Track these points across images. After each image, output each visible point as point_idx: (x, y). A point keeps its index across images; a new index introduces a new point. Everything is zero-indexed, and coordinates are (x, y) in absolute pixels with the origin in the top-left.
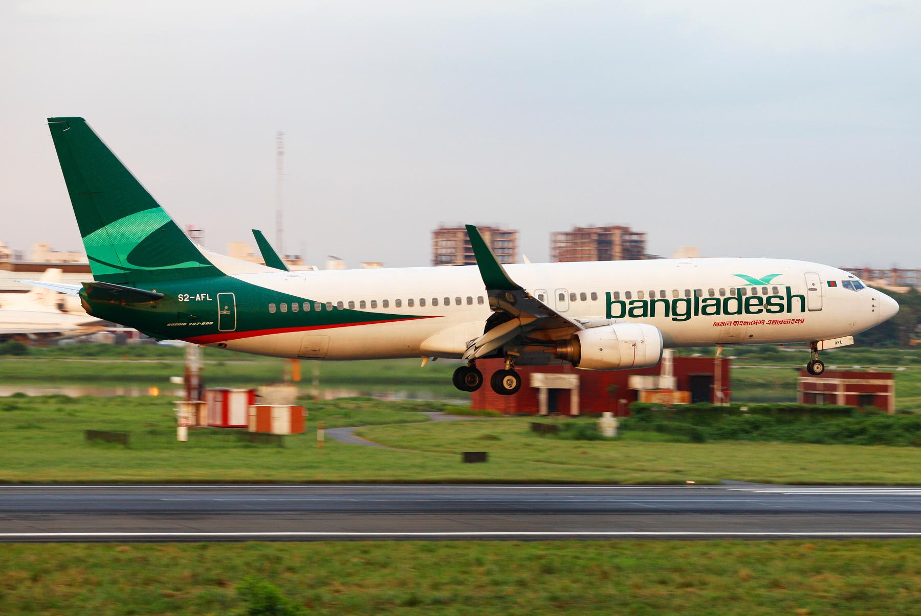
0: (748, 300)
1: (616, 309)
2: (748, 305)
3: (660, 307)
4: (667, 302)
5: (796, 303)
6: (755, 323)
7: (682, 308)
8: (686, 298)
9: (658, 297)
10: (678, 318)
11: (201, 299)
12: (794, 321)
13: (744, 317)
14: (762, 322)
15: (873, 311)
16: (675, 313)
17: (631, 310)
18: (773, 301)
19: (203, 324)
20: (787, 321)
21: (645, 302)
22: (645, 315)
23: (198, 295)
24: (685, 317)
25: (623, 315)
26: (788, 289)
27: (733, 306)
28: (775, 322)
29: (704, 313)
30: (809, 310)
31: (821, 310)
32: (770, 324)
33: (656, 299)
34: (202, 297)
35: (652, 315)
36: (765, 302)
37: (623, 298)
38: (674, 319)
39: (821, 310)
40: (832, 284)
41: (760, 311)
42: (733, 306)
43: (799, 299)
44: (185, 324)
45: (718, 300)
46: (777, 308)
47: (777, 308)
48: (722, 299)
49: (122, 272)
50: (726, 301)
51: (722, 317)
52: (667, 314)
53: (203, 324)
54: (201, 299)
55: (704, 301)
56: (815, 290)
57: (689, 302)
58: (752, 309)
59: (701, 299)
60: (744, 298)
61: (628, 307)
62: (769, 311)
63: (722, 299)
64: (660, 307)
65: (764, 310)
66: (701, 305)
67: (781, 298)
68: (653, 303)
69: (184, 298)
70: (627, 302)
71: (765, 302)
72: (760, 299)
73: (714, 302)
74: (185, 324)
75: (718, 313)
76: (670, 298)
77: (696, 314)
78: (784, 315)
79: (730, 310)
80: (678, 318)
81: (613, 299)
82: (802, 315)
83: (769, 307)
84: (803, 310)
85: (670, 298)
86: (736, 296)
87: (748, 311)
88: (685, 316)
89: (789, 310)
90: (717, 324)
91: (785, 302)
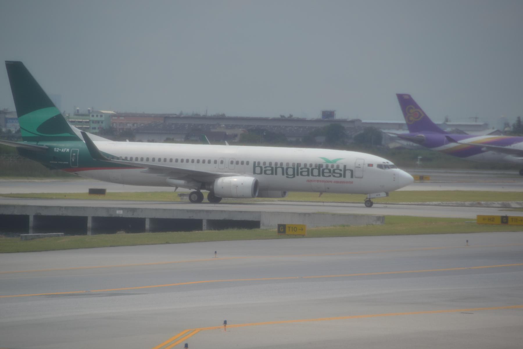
0: (323, 170)
1: (258, 170)
2: (323, 172)
3: (279, 170)
4: (283, 169)
5: (348, 174)
6: (328, 182)
7: (290, 171)
8: (292, 167)
9: (279, 165)
10: (289, 176)
11: (64, 150)
12: (347, 182)
13: (321, 178)
14: (331, 182)
15: (394, 180)
16: (287, 174)
17: (265, 171)
18: (336, 171)
19: (64, 163)
20: (344, 182)
21: (272, 168)
22: (272, 174)
23: (63, 149)
24: (292, 176)
25: (261, 173)
26: (345, 166)
27: (316, 172)
28: (337, 182)
29: (302, 175)
30: (356, 177)
31: (362, 178)
32: (335, 183)
33: (277, 167)
34: (65, 150)
35: (276, 174)
36: (332, 172)
37: (261, 165)
38: (287, 177)
39: (362, 178)
40: (370, 165)
41: (330, 176)
42: (316, 172)
43: (350, 171)
44: (56, 162)
45: (308, 169)
46: (338, 175)
47: (338, 175)
48: (310, 169)
49: (37, 136)
50: (312, 169)
51: (311, 178)
52: (283, 174)
53: (64, 163)
54: (64, 150)
55: (301, 169)
56: (360, 167)
57: (294, 169)
58: (325, 174)
59: (299, 168)
60: (321, 169)
61: (264, 169)
62: (334, 176)
63: (310, 169)
64: (279, 170)
65: (332, 176)
66: (300, 171)
67: (341, 170)
68: (276, 168)
69: (57, 150)
70: (263, 167)
71: (332, 172)
72: (330, 170)
73: (306, 170)
74: (56, 162)
75: (308, 175)
76: (285, 166)
77: (298, 175)
78: (342, 179)
79: (314, 174)
80: (289, 176)
81: (256, 165)
82: (351, 180)
83: (334, 174)
84: (352, 176)
85: (285, 166)
86: (318, 168)
87: (323, 175)
88: (292, 176)
89: (345, 176)
90: (308, 181)
91: (342, 173)
